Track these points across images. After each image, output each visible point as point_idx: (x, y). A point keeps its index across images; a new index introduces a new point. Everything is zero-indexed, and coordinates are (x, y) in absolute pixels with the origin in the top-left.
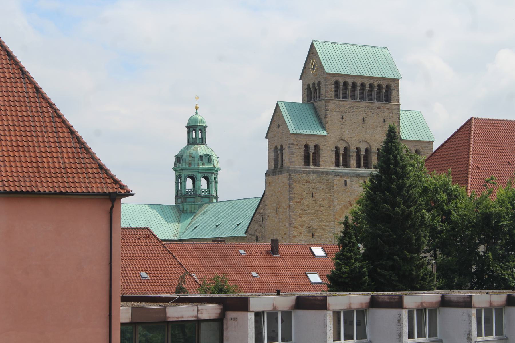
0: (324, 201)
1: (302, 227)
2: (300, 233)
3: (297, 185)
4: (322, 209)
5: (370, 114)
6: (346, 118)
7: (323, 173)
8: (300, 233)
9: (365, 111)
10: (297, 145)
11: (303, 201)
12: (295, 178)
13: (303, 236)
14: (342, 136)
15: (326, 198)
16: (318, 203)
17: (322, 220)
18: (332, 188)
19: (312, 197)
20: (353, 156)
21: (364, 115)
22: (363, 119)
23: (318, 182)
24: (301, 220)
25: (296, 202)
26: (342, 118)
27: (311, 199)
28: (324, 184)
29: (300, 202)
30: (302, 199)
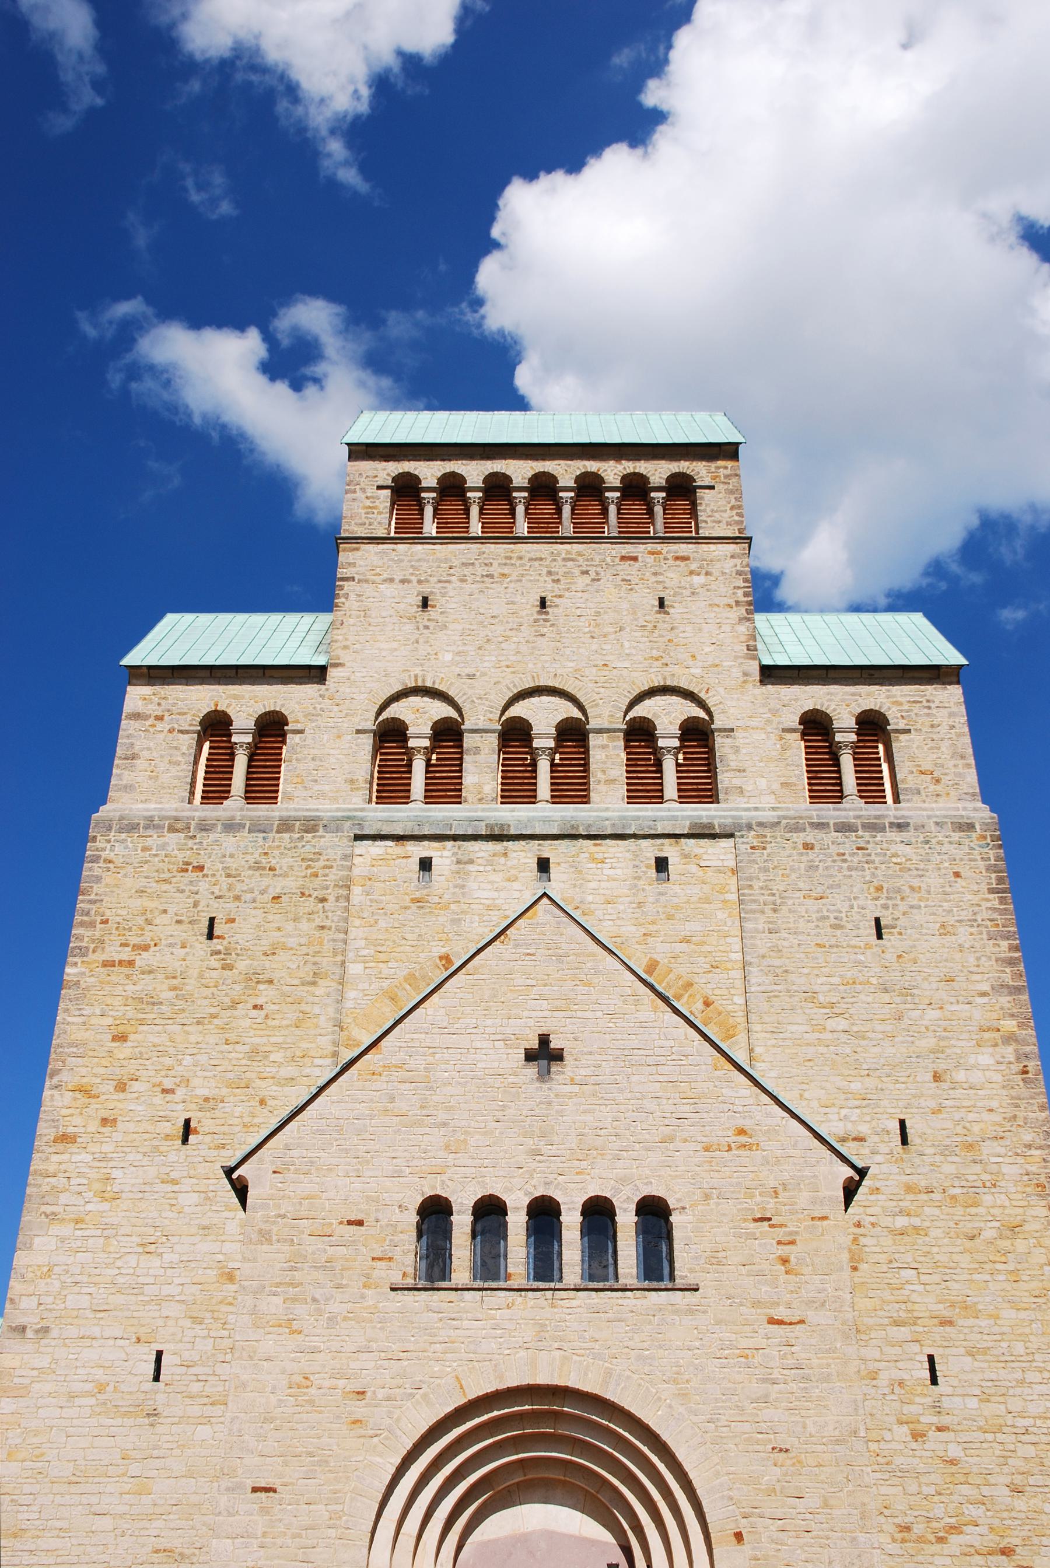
0: (282, 956)
1: (121, 1087)
2: (104, 1121)
3: (129, 882)
4: (265, 994)
5: (583, 581)
6: (448, 602)
7: (285, 826)
8: (104, 1121)
9: (550, 573)
10: (159, 718)
11: (143, 960)
12: (119, 848)
13: (118, 1136)
14: (417, 670)
15: (292, 942)
16: (242, 965)
17: (255, 1054)
18: (331, 895)
19: (210, 936)
20: (477, 750)
21: (550, 585)
22: (543, 603)
23: (257, 867)
24: (123, 1051)
25: (106, 964)
26: (425, 603)
27: (202, 946)
28: (285, 875)
29: (131, 963)
30: (146, 948)
